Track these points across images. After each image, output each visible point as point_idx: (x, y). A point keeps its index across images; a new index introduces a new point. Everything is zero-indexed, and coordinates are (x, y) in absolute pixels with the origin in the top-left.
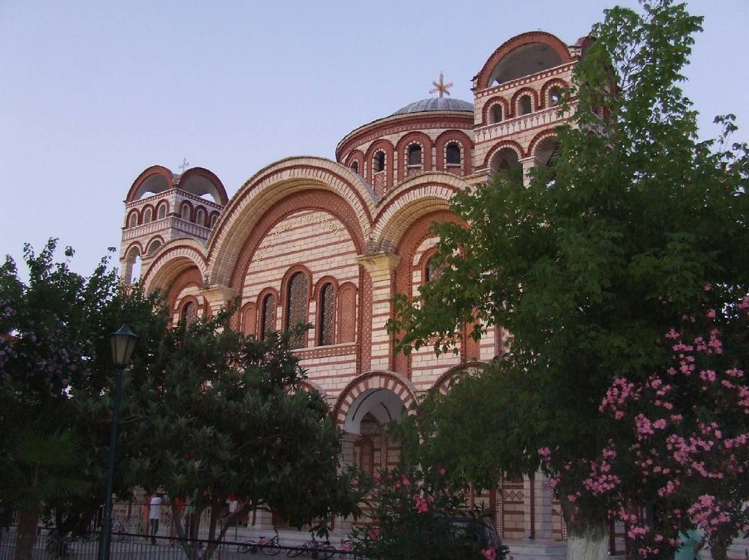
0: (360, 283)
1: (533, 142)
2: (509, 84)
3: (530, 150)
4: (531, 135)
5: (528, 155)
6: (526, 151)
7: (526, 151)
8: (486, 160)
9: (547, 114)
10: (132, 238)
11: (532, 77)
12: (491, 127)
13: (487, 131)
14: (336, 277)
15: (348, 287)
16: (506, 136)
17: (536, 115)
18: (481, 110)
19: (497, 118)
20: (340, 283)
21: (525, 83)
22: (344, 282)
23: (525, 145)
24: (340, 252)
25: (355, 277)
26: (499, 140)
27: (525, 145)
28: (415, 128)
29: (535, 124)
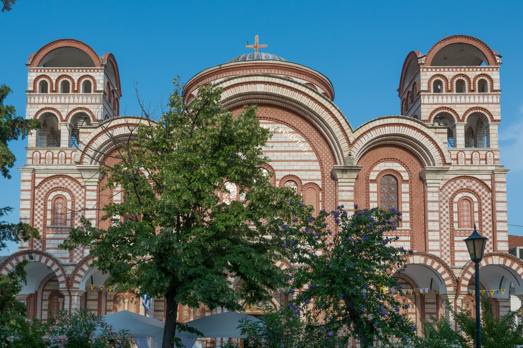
0: (322, 184)
1: (467, 112)
2: (449, 68)
3: (464, 117)
4: (465, 108)
5: (463, 120)
6: (461, 118)
7: (461, 118)
8: (430, 117)
9: (477, 97)
10: (77, 104)
11: (466, 68)
12: (444, 95)
13: (486, 97)
14: (300, 177)
15: (315, 187)
16: (449, 104)
17: (468, 95)
18: (427, 81)
19: (436, 90)
20: (304, 183)
21: (465, 71)
22: (307, 182)
23: (461, 114)
24: (303, 159)
25: (319, 180)
26: (441, 106)
27: (461, 114)
28: (315, 82)
29: (436, 101)
